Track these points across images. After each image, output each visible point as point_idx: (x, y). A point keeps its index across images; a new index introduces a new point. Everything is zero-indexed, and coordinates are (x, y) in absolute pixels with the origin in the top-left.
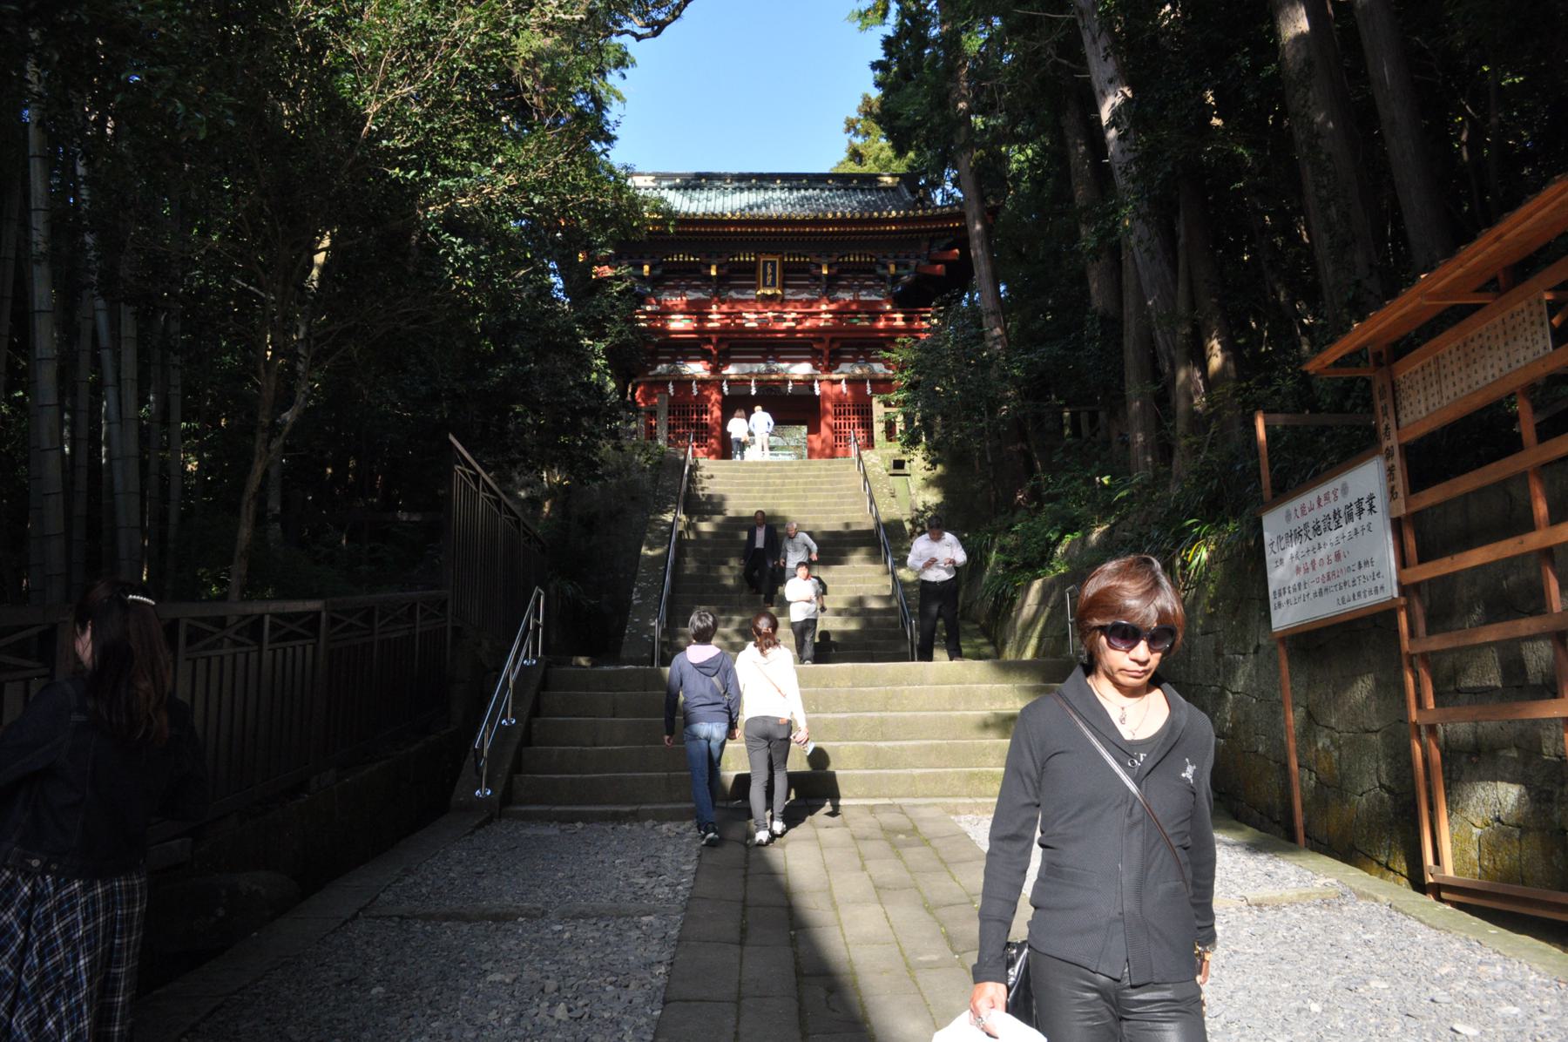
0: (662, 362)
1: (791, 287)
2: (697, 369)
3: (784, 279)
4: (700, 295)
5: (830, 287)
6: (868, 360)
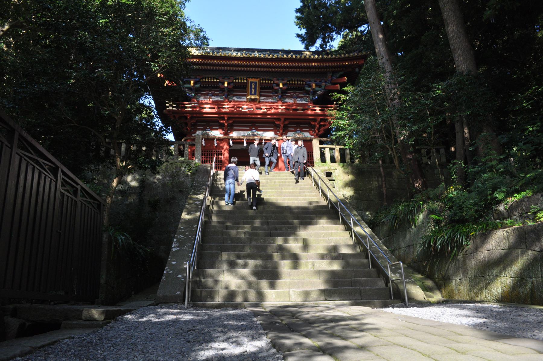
0: (199, 129)
1: (264, 96)
2: (217, 133)
3: (261, 92)
4: (219, 99)
5: (283, 95)
6: (302, 131)
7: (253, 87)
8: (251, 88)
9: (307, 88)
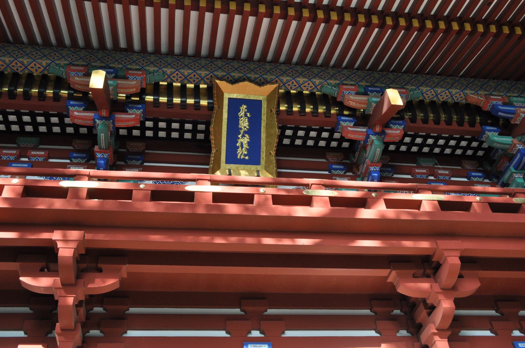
7: (244, 124)
9: (494, 137)
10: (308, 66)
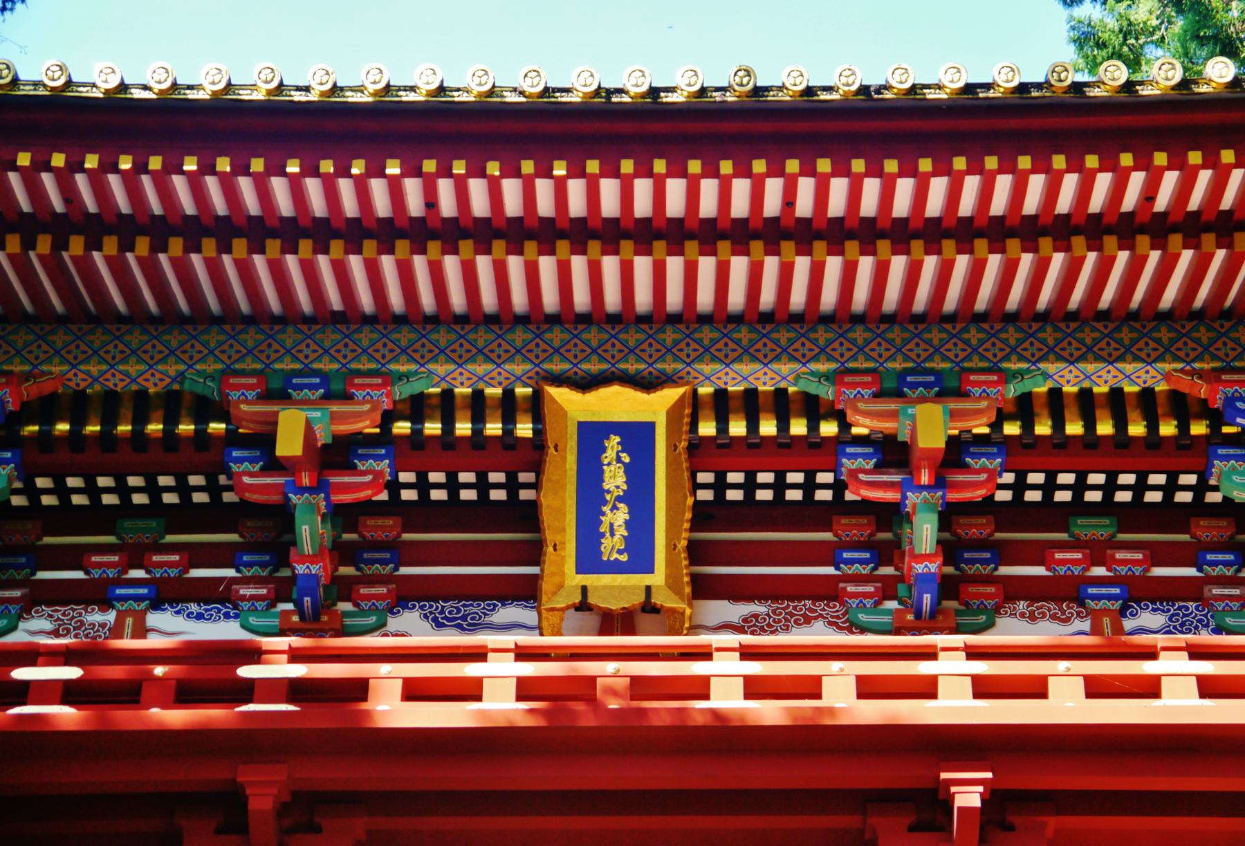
7: (615, 479)
8: (591, 497)
10: (765, 327)
